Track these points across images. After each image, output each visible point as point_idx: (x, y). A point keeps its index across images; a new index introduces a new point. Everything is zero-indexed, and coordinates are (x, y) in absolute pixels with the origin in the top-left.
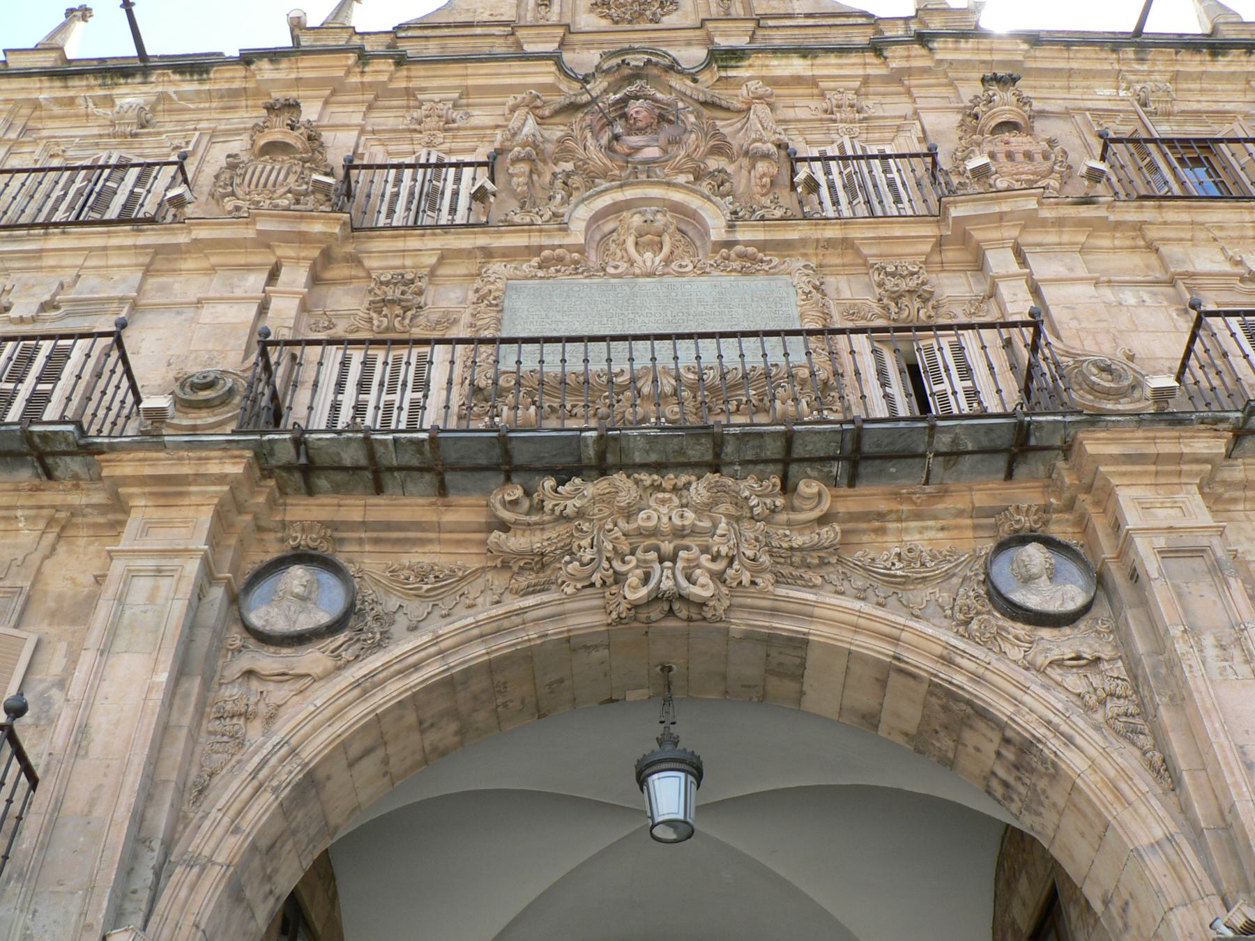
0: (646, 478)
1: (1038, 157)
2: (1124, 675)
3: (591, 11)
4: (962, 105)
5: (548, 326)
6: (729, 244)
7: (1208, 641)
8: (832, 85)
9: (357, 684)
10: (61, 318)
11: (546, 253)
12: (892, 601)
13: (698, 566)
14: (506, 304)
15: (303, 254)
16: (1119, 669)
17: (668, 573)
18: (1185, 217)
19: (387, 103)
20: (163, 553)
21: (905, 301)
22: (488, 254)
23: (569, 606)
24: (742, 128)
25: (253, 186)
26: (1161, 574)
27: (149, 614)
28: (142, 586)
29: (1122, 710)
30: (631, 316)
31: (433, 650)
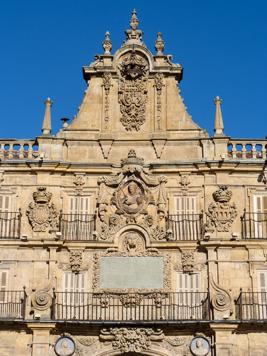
5: (110, 273)
6: (150, 247)
17: (132, 348)
18: (256, 243)
30: (128, 270)
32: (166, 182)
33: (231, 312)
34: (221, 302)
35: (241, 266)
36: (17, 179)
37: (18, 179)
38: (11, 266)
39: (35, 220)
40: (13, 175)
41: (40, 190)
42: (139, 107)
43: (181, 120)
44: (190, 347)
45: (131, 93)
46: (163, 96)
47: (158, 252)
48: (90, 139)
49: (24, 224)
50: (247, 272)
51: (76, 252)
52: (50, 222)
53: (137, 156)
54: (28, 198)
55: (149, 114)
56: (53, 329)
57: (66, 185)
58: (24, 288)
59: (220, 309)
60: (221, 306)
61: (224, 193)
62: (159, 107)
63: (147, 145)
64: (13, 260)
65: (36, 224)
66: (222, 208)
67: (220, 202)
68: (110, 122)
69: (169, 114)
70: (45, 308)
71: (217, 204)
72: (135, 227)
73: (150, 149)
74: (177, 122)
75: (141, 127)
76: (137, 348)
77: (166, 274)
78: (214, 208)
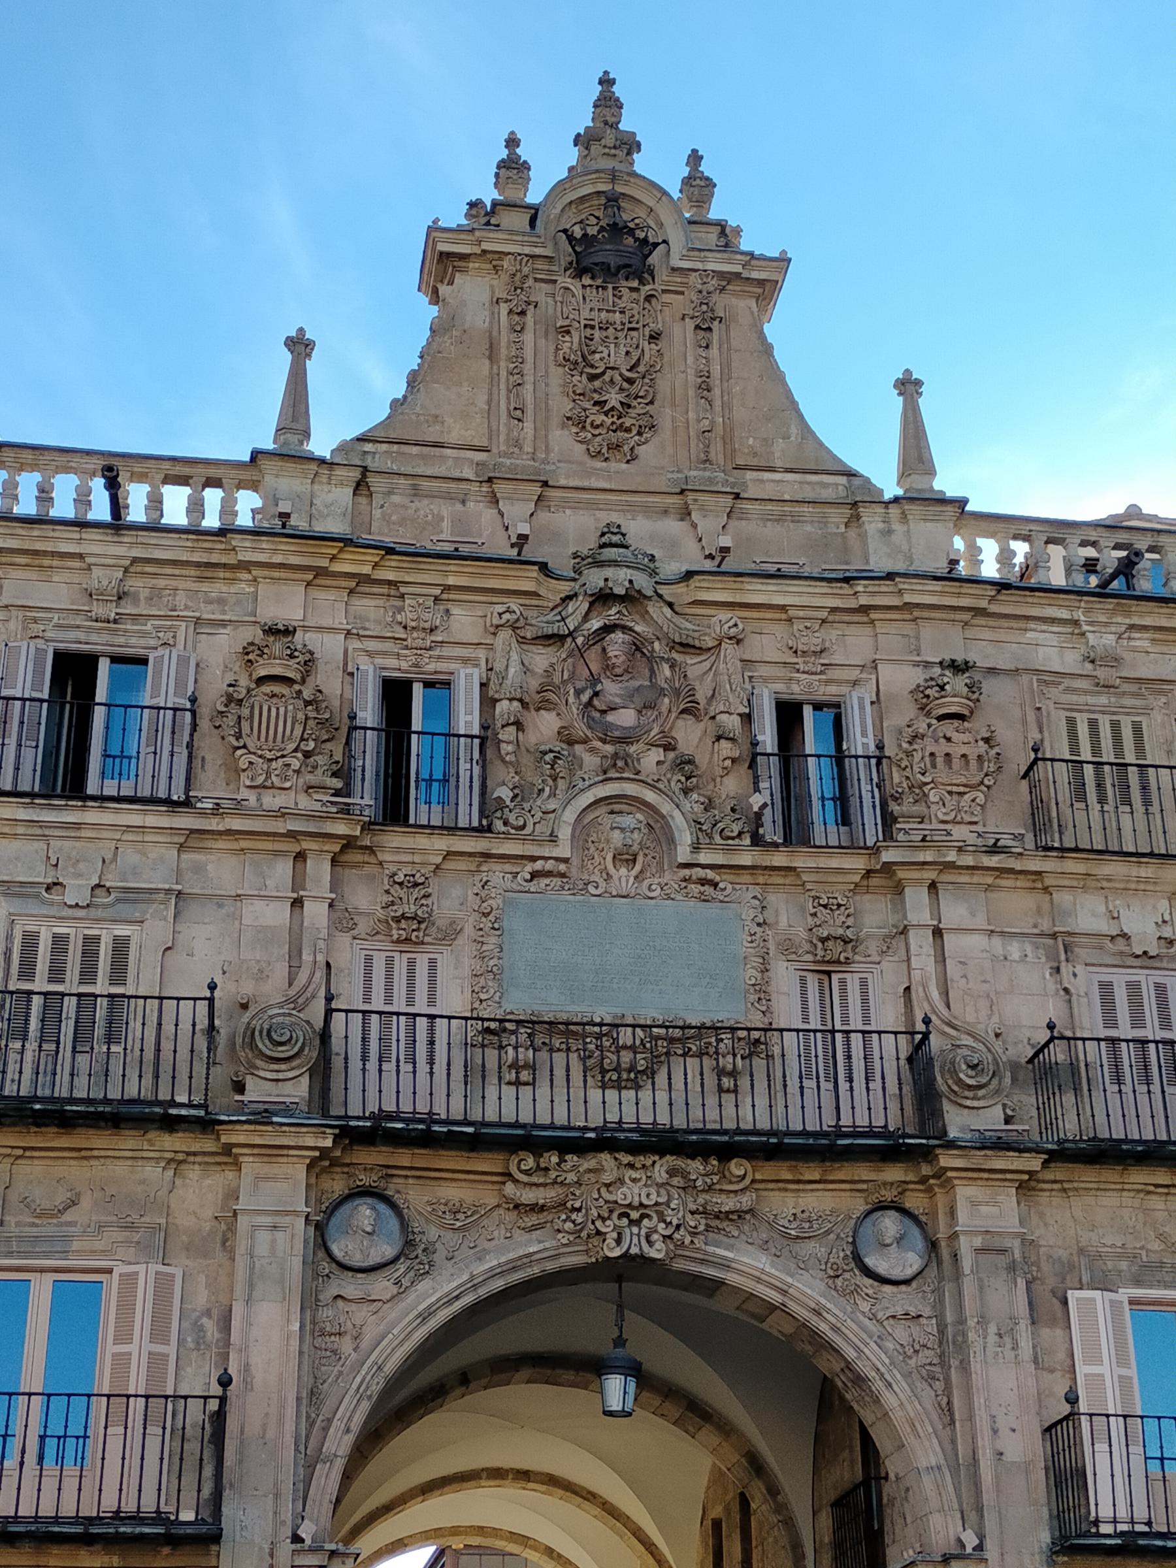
0: (626, 1158)
1: (973, 763)
2: (935, 1332)
3: (563, 426)
4: (918, 659)
7: (992, 1329)
8: (801, 614)
9: (420, 1315)
10: (113, 905)
11: (539, 865)
12: (786, 1252)
13: (656, 1231)
14: (505, 924)
15: (325, 848)
16: (932, 1326)
17: (635, 1240)
18: (1081, 868)
19: (367, 590)
20: (277, 1213)
21: (830, 944)
22: (487, 856)
23: (562, 1250)
24: (710, 669)
25: (263, 739)
26: (972, 1271)
27: (274, 1265)
28: (263, 1237)
29: (928, 1361)
30: (608, 946)
31: (469, 1285)
32: (739, 642)
33: (1010, 1113)
34: (971, 1072)
35: (1029, 949)
36: (177, 598)
37: (181, 599)
38: (151, 911)
39: (251, 746)
40: (161, 583)
41: (272, 631)
42: (631, 381)
43: (786, 437)
44: (854, 1243)
45: (604, 334)
46: (714, 352)
47: (721, 885)
48: (457, 474)
49: (203, 759)
50: (1051, 974)
51: (408, 870)
52: (307, 755)
53: (630, 540)
54: (222, 667)
55: (668, 411)
56: (324, 1152)
57: (365, 629)
58: (212, 987)
59: (968, 1103)
60: (970, 1087)
61: (958, 684)
62: (704, 387)
63: (666, 512)
64: (160, 886)
65: (253, 758)
66: (949, 740)
67: (940, 718)
68: (528, 425)
69: (739, 414)
70: (290, 1074)
71: (929, 726)
72: (631, 789)
73: (673, 526)
74: (767, 442)
75: (638, 450)
76: (650, 1243)
77: (753, 967)
78: (916, 737)
